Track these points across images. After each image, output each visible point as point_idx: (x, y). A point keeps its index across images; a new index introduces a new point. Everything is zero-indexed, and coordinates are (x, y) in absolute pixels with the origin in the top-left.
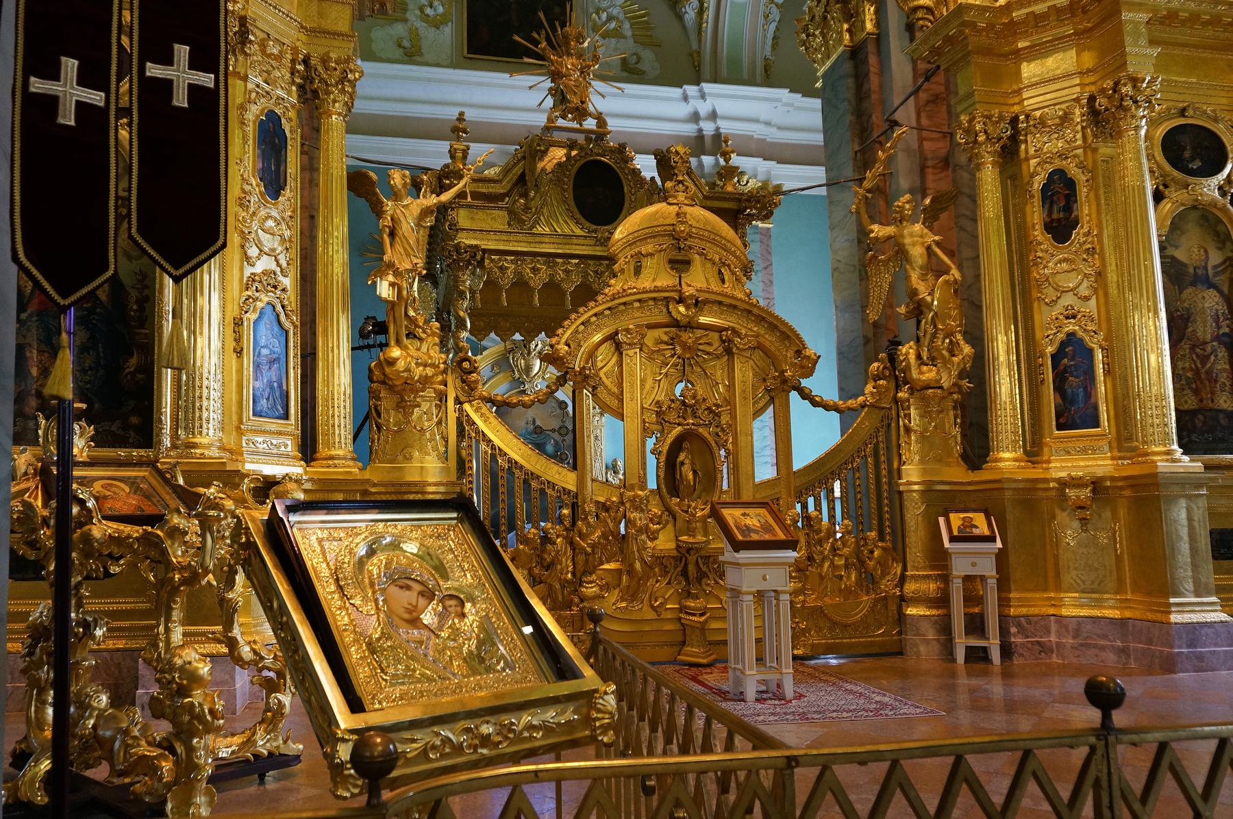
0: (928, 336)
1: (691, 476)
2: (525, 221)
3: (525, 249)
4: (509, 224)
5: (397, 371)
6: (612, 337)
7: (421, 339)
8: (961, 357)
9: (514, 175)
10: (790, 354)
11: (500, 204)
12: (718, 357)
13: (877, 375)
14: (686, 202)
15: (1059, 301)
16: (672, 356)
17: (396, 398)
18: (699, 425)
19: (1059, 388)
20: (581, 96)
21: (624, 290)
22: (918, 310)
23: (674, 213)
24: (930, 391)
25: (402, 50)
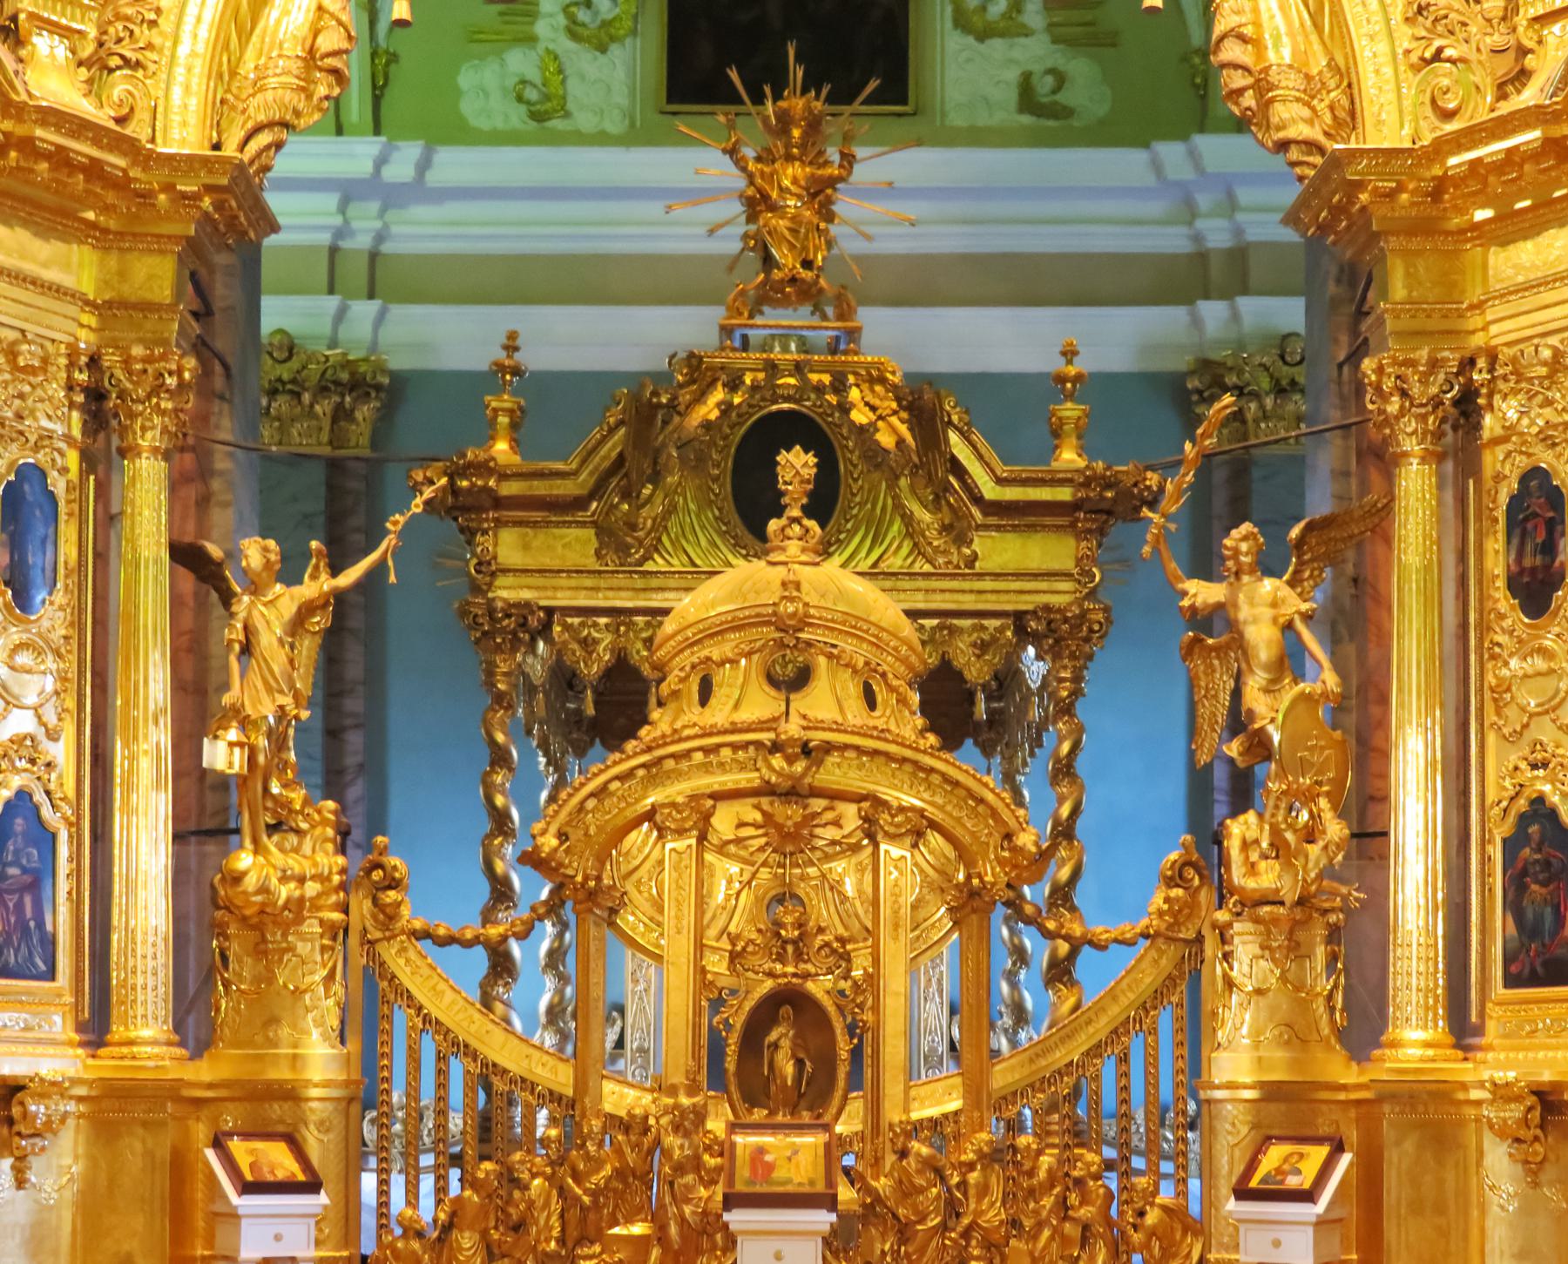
0: (1271, 803)
1: (789, 1069)
2: (629, 547)
3: (630, 604)
4: (598, 554)
5: (245, 893)
6: (650, 815)
7: (298, 832)
8: (1321, 843)
9: (604, 458)
10: (997, 837)
11: (581, 516)
12: (856, 848)
13: (1171, 878)
14: (804, 558)
15: (1526, 733)
16: (761, 849)
17: (253, 936)
18: (806, 976)
19: (1514, 905)
20: (805, 248)
21: (675, 731)
22: (1260, 746)
23: (778, 582)
24: (1267, 909)
25: (523, 108)
